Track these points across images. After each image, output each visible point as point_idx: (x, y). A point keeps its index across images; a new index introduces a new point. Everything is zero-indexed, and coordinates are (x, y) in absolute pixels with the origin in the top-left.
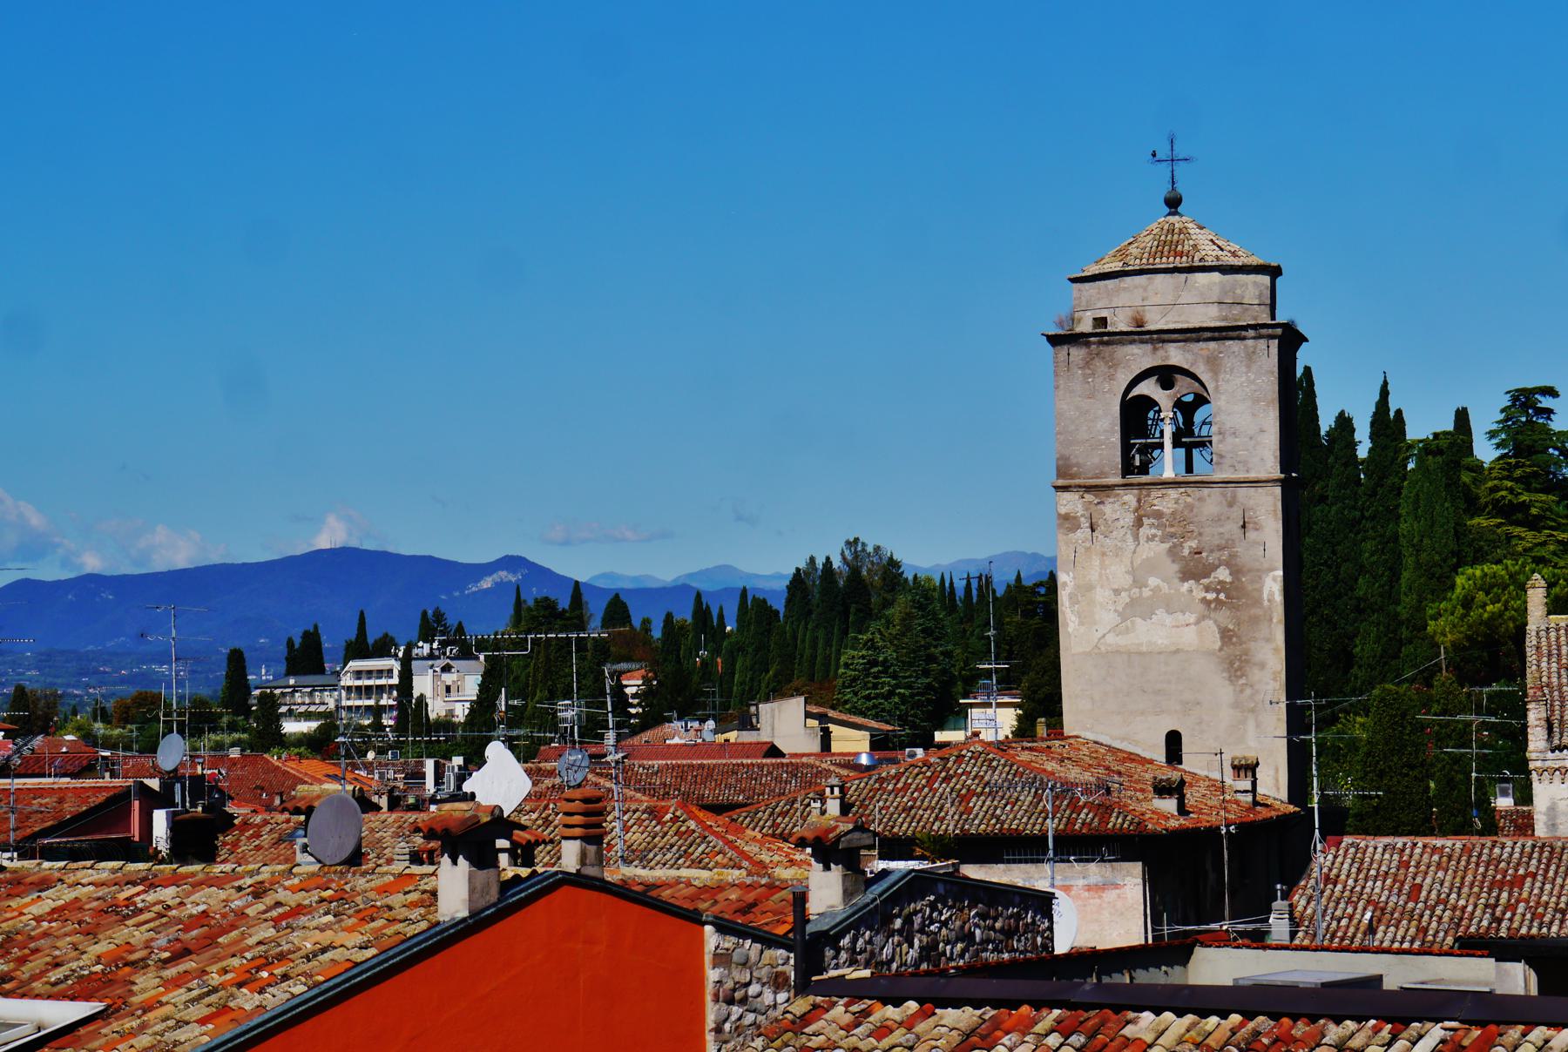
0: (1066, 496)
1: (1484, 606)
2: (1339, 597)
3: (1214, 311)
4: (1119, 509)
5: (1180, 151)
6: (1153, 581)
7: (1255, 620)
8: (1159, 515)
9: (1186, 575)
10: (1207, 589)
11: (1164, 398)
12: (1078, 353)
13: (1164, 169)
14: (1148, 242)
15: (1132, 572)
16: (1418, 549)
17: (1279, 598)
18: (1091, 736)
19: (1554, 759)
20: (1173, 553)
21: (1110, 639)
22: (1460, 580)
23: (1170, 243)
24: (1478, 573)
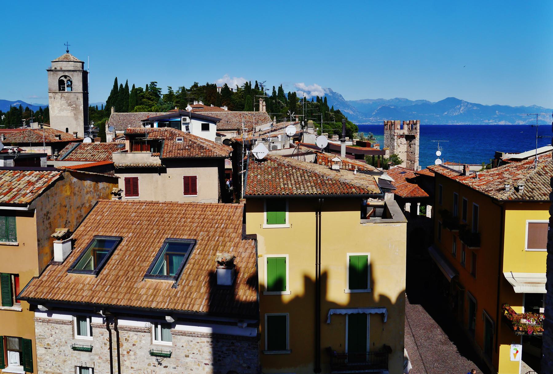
2: (120, 109)
3: (73, 68)
4: (58, 96)
5: (68, 44)
7: (79, 112)
8: (64, 97)
10: (72, 108)
11: (65, 80)
12: (51, 73)
13: (66, 47)
14: (63, 57)
17: (82, 109)
21: (57, 114)
22: (135, 108)
23: (65, 58)
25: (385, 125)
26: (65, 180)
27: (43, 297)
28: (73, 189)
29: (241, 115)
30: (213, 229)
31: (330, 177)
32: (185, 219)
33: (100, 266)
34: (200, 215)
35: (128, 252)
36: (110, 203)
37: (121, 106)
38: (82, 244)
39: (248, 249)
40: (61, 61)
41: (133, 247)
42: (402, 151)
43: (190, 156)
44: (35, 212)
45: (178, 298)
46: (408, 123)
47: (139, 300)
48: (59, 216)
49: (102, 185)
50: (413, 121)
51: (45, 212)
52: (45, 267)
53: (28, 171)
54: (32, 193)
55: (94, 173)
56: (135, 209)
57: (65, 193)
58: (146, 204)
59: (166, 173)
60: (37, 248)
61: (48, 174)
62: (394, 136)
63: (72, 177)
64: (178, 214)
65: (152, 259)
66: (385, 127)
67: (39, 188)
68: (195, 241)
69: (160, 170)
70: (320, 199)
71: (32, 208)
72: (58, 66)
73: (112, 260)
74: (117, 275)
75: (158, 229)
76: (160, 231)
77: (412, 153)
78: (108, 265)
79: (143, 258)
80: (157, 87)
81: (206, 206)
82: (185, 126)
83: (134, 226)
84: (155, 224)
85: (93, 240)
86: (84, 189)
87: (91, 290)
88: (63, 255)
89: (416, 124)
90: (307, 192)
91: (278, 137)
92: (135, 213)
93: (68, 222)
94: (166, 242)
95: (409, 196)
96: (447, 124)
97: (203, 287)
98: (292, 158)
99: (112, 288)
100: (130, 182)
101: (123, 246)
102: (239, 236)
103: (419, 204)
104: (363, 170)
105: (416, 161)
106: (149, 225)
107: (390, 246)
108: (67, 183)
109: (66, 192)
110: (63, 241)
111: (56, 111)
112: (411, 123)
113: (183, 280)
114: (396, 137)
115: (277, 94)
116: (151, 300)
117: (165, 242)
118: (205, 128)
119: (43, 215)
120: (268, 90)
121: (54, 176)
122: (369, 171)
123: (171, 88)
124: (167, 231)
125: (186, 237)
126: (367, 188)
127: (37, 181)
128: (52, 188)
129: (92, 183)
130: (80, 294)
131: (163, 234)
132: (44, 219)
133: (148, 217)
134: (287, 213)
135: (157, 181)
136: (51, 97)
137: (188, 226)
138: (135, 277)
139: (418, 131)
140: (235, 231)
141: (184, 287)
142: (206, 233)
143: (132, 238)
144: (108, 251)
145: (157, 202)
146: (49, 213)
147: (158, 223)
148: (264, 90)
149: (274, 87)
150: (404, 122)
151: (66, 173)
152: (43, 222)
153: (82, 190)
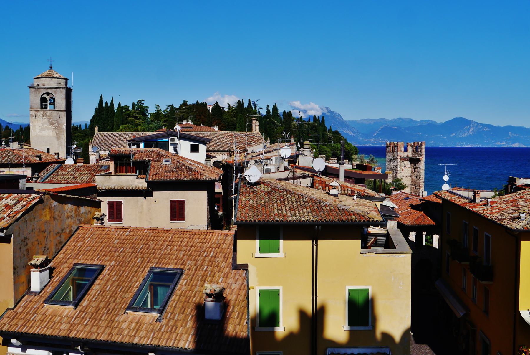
0: (32, 112)
4: (40, 114)
5: (52, 60)
6: (45, 125)
7: (61, 132)
8: (46, 115)
9: (51, 124)
10: (54, 127)
11: (48, 97)
12: (34, 90)
13: (50, 62)
14: (46, 73)
15: (42, 124)
16: (116, 122)
17: (65, 128)
18: (35, 148)
20: (49, 121)
21: (38, 134)
22: (121, 127)
23: (49, 74)
25: (388, 147)
26: (45, 204)
27: (17, 330)
28: (53, 213)
29: (232, 135)
30: (201, 258)
31: (328, 202)
32: (172, 246)
33: (79, 296)
34: (188, 242)
35: (110, 282)
36: (92, 229)
37: (106, 125)
38: (61, 272)
39: (239, 280)
40: (44, 78)
41: (115, 277)
43: (178, 178)
44: (12, 238)
45: (163, 333)
46: (412, 144)
47: (120, 335)
48: (37, 242)
49: (84, 209)
50: (418, 143)
51: (23, 238)
52: (20, 297)
53: (6, 194)
54: (10, 217)
55: (76, 197)
56: (118, 235)
57: (44, 217)
58: (130, 230)
59: (152, 196)
60: (13, 277)
61: (27, 197)
62: (397, 159)
63: (52, 201)
64: (164, 241)
65: (135, 290)
66: (388, 149)
67: (17, 212)
68: (182, 270)
69: (146, 194)
70: (316, 227)
71: (9, 233)
72: (41, 82)
73: (92, 290)
74: (97, 307)
75: (142, 257)
76: (144, 259)
77: (417, 177)
78: (88, 295)
79: (125, 289)
80: (144, 105)
81: (194, 233)
83: (117, 254)
84: (139, 252)
85: (73, 269)
86: (64, 214)
87: (69, 323)
88: (40, 285)
89: (421, 146)
90: (303, 219)
91: (272, 160)
92: (118, 239)
93: (46, 249)
94: (151, 271)
95: (414, 224)
96: (455, 146)
97: (190, 321)
98: (287, 181)
99: (92, 321)
100: (113, 206)
101: (105, 276)
102: (229, 266)
103: (425, 233)
104: (363, 196)
105: (421, 186)
106: (132, 252)
107: (393, 279)
108: (47, 207)
109: (46, 216)
110: (41, 269)
111: (38, 131)
112: (416, 145)
113: (168, 314)
114: (399, 160)
115: (271, 113)
116: (133, 334)
117: (149, 272)
119: (21, 241)
120: (262, 108)
121: (33, 199)
122: (370, 196)
123: (158, 106)
124: (152, 259)
125: (172, 266)
126: (367, 215)
127: (15, 204)
128: (31, 212)
129: (74, 207)
130: (57, 327)
131: (148, 263)
132: (21, 245)
133: (132, 244)
134: (281, 242)
135: (142, 205)
136: (32, 116)
137: (174, 254)
138: (116, 309)
139: (424, 153)
140: (225, 261)
141: (169, 320)
142: (194, 262)
143: (114, 267)
144: (88, 280)
145: (142, 228)
146: (26, 239)
147: (143, 251)
148: (257, 109)
149: (268, 106)
150: (407, 143)
151: (46, 196)
152: (20, 248)
153: (63, 215)
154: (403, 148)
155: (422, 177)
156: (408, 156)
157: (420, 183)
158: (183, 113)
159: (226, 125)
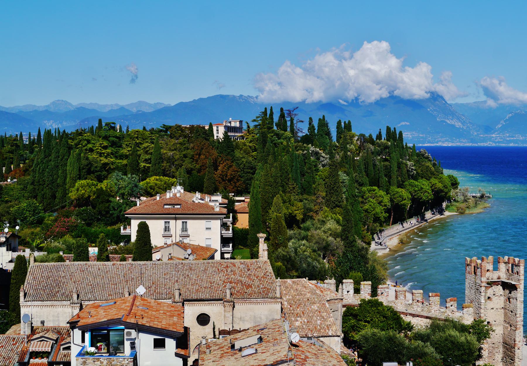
1: (81, 191)
2: (53, 183)
19: (25, 304)
22: (76, 184)
24: (80, 183)
29: (227, 267)
42: (496, 306)
50: (514, 261)
62: (481, 287)
77: (512, 312)
82: (129, 342)
105: (518, 326)
112: (511, 261)
115: (316, 131)
118: (159, 344)
120: (302, 122)
139: (522, 277)
148: (295, 122)
149: (311, 119)
154: (492, 266)
155: (520, 314)
156: (499, 278)
157: (517, 322)
158: (173, 150)
159: (240, 168)
